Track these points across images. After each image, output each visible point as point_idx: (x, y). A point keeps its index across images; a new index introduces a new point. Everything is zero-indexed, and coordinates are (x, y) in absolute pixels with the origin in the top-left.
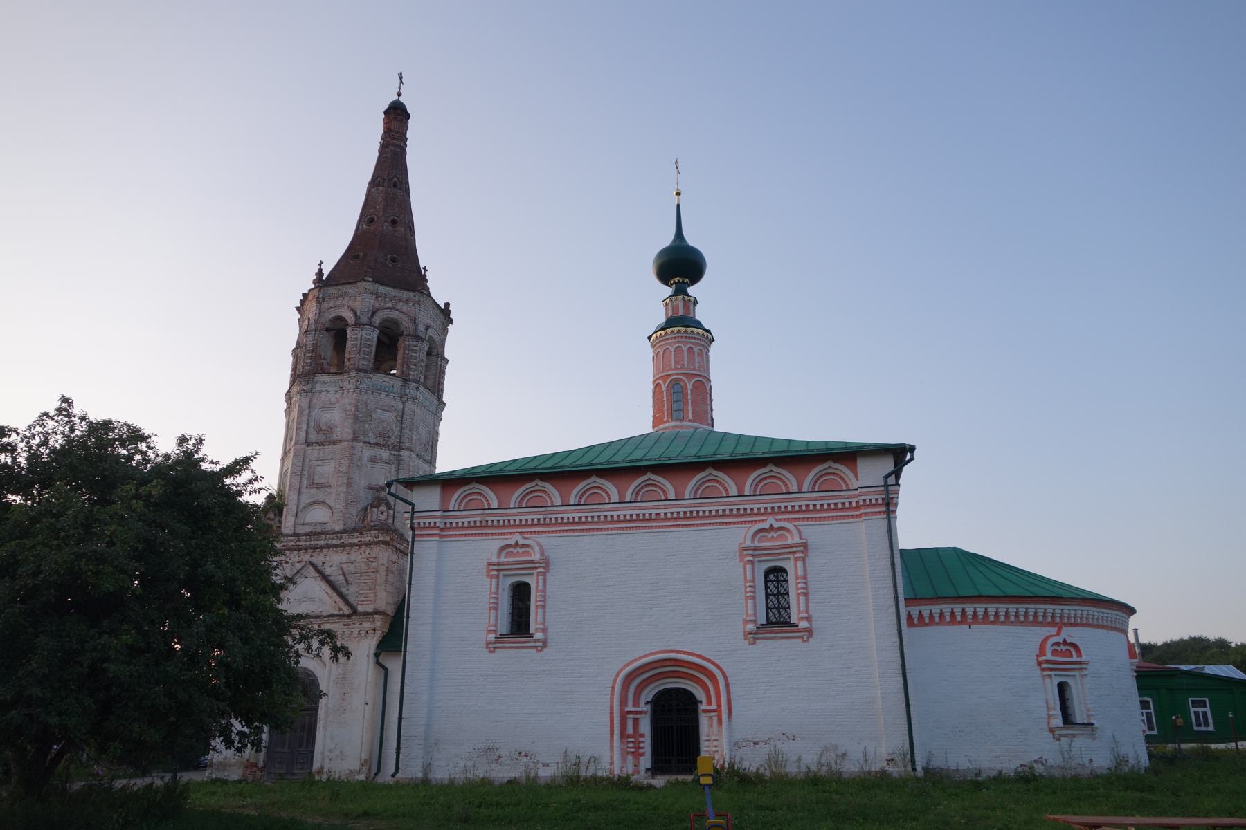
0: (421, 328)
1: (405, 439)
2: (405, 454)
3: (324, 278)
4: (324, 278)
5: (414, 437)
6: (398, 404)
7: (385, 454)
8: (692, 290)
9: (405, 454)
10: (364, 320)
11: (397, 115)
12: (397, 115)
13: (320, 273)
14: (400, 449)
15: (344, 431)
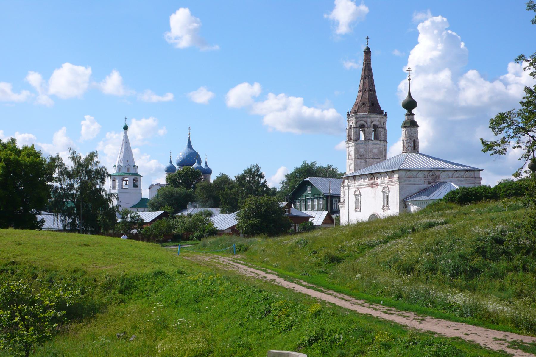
0: (369, 124)
1: (367, 156)
2: (367, 160)
3: (349, 113)
4: (349, 113)
5: (370, 154)
6: (364, 146)
7: (363, 161)
8: (414, 111)
9: (367, 160)
10: (355, 126)
11: (368, 52)
12: (368, 52)
13: (348, 112)
14: (366, 159)
15: (353, 157)
